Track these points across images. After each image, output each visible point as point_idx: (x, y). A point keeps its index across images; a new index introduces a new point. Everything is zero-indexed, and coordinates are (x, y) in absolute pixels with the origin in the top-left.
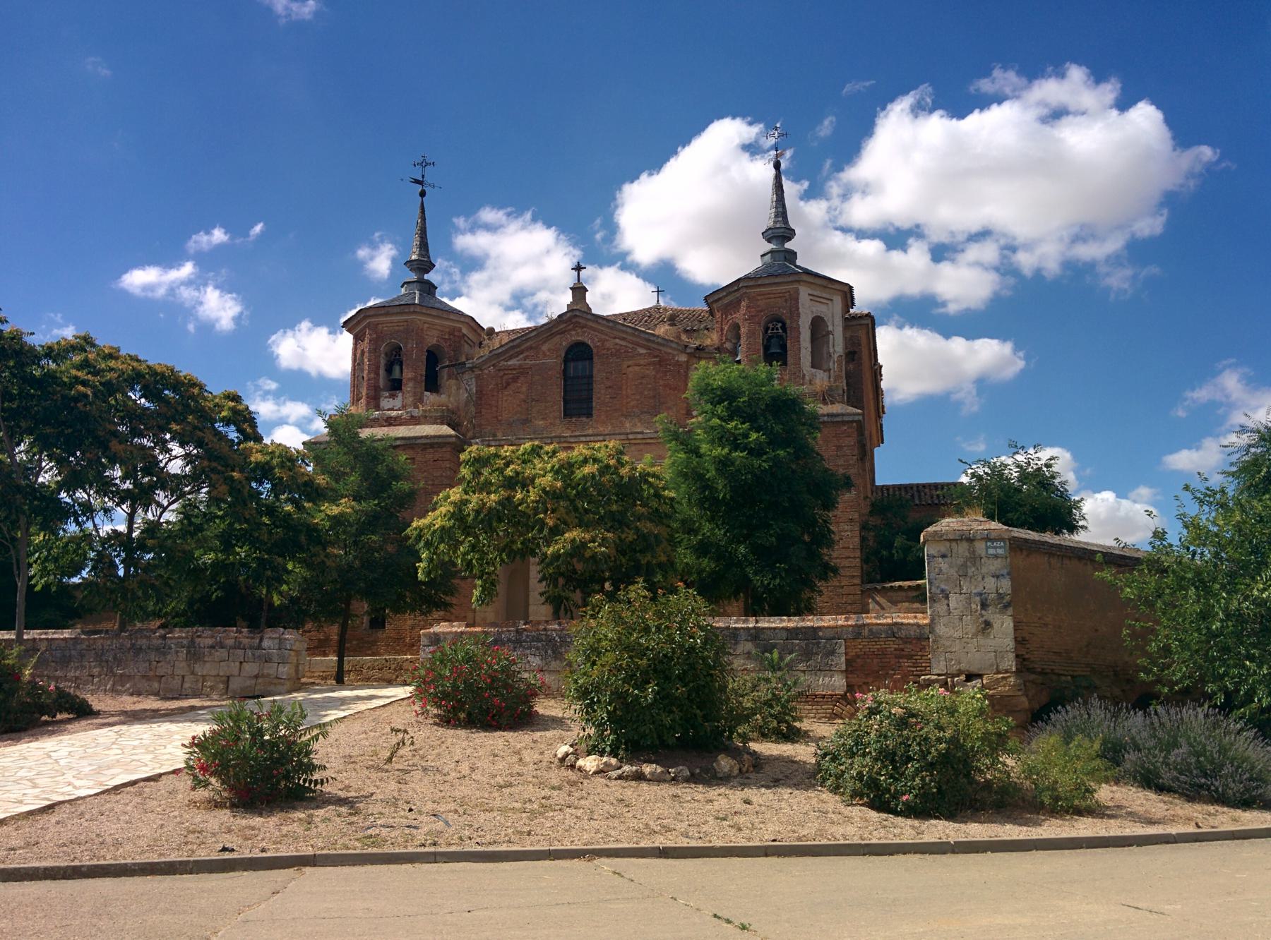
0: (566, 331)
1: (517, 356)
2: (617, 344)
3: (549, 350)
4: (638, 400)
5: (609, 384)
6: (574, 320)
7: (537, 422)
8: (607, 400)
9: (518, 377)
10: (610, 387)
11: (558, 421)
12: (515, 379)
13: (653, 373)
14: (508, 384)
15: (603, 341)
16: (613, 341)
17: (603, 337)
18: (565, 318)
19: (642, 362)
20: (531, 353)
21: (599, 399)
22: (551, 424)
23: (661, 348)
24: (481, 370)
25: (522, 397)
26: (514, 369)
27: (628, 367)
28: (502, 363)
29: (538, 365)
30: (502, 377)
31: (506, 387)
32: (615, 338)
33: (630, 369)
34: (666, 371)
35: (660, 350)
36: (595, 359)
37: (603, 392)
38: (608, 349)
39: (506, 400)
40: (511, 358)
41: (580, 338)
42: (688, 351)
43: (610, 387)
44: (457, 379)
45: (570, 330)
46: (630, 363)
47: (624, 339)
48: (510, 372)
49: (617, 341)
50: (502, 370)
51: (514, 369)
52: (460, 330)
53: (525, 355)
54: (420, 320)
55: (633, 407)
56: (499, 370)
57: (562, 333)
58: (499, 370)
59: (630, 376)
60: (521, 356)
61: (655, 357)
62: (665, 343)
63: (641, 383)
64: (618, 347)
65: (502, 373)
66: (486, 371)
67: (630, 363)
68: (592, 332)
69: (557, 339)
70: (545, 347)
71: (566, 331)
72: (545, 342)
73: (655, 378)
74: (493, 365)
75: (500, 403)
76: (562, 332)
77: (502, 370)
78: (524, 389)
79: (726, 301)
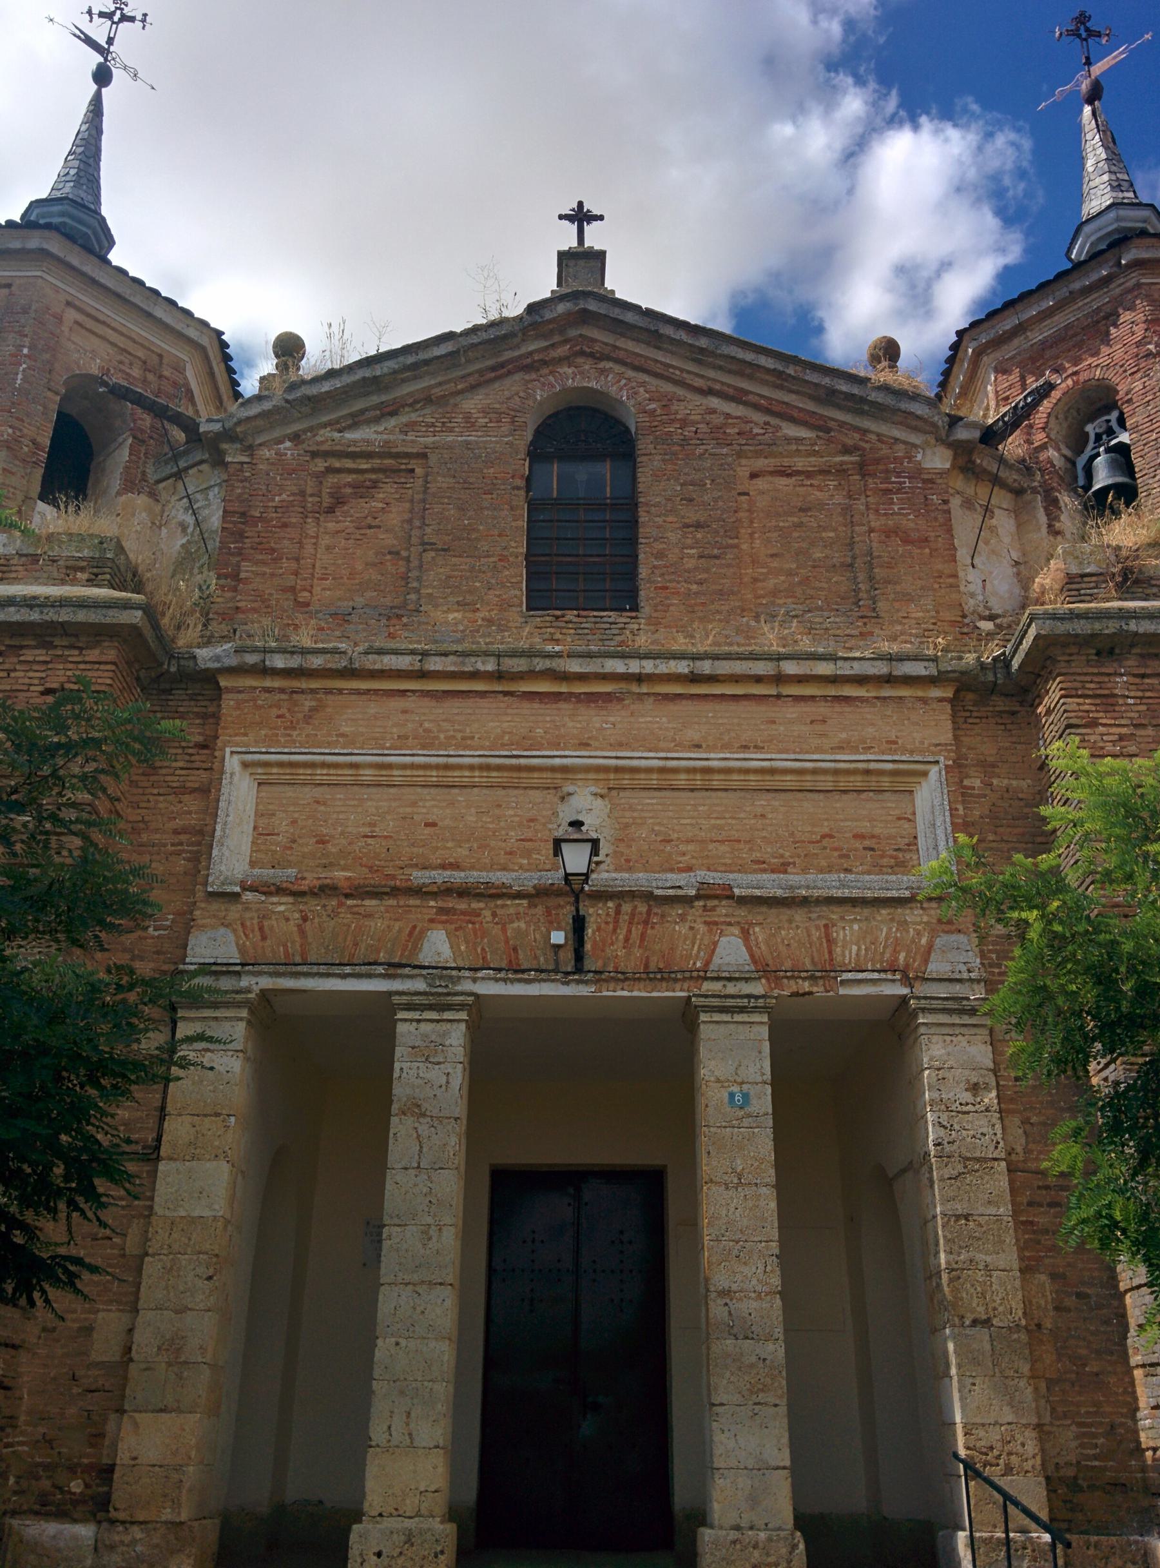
0: (545, 363)
1: (377, 420)
2: (713, 411)
3: (485, 412)
4: (790, 573)
5: (692, 516)
6: (573, 333)
7: (438, 615)
8: (690, 564)
9: (375, 485)
10: (698, 526)
11: (515, 616)
12: (364, 490)
13: (839, 499)
14: (339, 501)
15: (667, 401)
16: (698, 399)
17: (668, 388)
18: (548, 315)
19: (800, 463)
20: (428, 415)
21: (660, 555)
22: (490, 621)
23: (866, 423)
24: (250, 449)
25: (388, 540)
26: (369, 455)
27: (753, 476)
28: (326, 434)
29: (450, 447)
30: (320, 477)
31: (331, 510)
32: (710, 392)
33: (761, 483)
34: (888, 491)
35: (865, 431)
36: (644, 445)
37: (673, 537)
38: (684, 423)
39: (328, 548)
40: (356, 421)
41: (593, 384)
42: (962, 434)
43: (698, 526)
44: (153, 495)
45: (560, 360)
46: (760, 463)
47: (738, 397)
48: (349, 464)
49: (714, 402)
50: (326, 454)
51: (369, 455)
52: (179, 368)
53: (404, 419)
54: (57, 290)
55: (775, 593)
56: (314, 454)
57: (527, 368)
58: (314, 454)
59: (762, 502)
60: (392, 422)
61: (846, 450)
62: (889, 400)
63: (800, 525)
64: (717, 420)
65: (320, 465)
66: (266, 453)
67: (760, 463)
68: (630, 373)
69: (513, 385)
70: (472, 404)
71: (545, 363)
72: (473, 388)
73: (846, 510)
74: (296, 438)
75: (309, 549)
76: (529, 366)
77: (326, 454)
78: (395, 517)
79: (1037, 336)
